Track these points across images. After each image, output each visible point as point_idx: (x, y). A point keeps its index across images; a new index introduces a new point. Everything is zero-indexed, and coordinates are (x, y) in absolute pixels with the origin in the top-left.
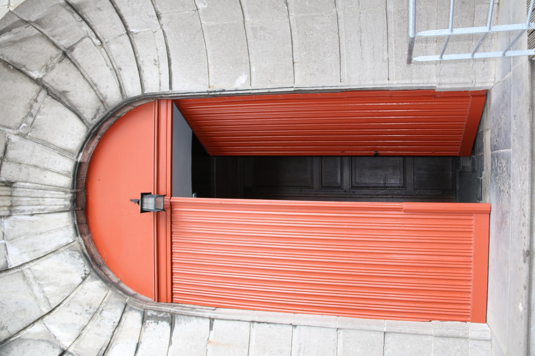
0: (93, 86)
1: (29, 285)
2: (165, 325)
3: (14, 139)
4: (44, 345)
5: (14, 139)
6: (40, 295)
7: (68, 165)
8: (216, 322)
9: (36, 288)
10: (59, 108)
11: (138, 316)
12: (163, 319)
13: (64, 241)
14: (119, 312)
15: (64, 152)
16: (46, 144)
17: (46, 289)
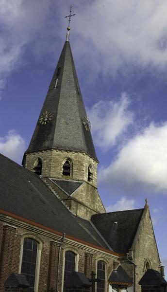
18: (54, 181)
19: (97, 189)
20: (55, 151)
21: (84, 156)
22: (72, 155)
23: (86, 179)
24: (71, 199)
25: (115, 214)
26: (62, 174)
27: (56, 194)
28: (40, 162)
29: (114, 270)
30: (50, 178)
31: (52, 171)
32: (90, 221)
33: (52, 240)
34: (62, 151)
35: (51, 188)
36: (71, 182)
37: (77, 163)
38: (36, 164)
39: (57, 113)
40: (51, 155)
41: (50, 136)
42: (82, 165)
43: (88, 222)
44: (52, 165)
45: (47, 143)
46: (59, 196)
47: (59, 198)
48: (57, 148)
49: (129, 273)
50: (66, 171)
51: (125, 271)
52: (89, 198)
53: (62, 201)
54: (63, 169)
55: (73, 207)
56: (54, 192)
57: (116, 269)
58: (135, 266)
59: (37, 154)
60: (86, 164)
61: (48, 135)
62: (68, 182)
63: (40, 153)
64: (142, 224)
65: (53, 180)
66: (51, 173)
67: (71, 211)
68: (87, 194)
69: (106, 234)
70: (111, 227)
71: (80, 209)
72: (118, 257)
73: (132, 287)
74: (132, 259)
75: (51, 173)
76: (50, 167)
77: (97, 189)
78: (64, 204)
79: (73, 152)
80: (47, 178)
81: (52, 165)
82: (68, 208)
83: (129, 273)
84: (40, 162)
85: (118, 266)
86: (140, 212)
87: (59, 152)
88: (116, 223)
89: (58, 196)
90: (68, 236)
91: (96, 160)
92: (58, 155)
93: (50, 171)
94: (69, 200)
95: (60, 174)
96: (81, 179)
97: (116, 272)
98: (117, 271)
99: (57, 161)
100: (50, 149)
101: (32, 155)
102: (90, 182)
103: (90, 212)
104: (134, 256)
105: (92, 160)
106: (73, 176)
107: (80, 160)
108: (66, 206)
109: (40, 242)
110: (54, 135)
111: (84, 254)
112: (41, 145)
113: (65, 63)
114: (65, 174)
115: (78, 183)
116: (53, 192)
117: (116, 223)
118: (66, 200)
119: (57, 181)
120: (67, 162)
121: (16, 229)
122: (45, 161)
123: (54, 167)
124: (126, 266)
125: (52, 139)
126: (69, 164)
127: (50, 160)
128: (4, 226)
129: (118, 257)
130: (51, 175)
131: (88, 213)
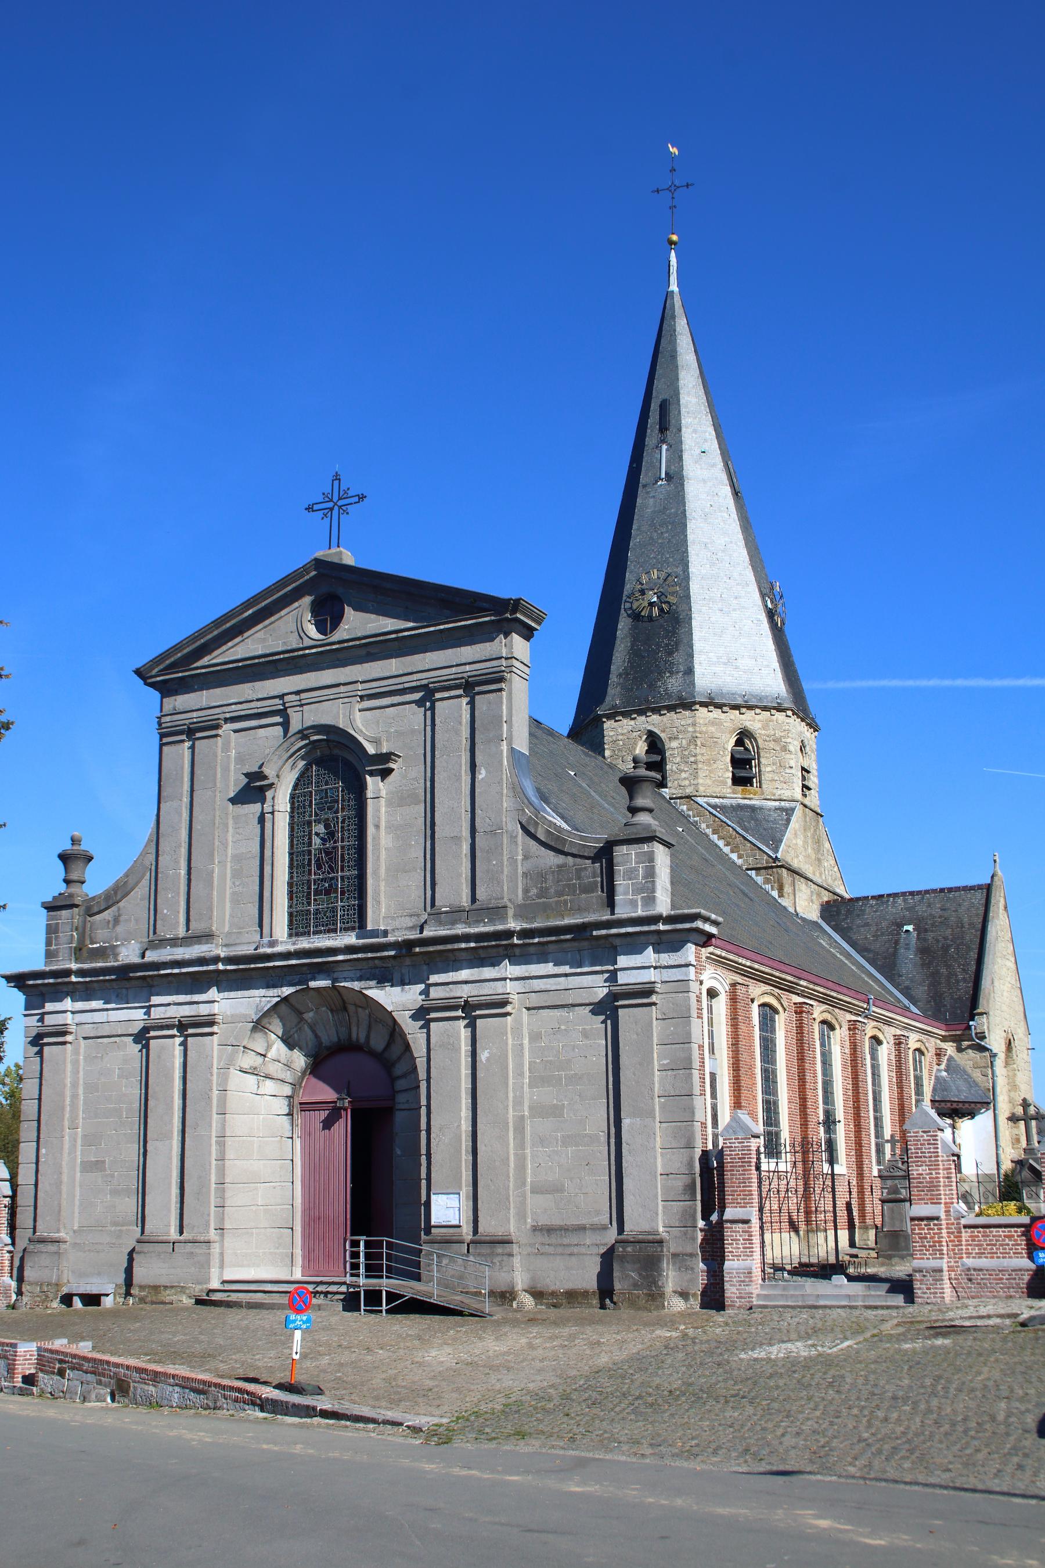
0: (399, 1058)
1: (296, 1026)
2: (286, 1111)
3: (367, 1011)
4: (266, 1044)
5: (367, 1011)
6: (291, 1033)
7: (362, 1040)
8: (290, 1140)
9: (295, 1030)
10: (387, 1038)
11: (290, 1094)
12: (290, 1109)
13: (323, 1041)
14: (290, 1081)
15: (368, 1037)
16: (370, 1027)
17: (296, 1035)
18: (715, 807)
19: (822, 816)
20: (703, 710)
21: (788, 720)
22: (752, 721)
23: (798, 794)
24: (782, 866)
25: (900, 900)
26: (730, 782)
27: (727, 850)
28: (655, 744)
29: (938, 1070)
30: (699, 800)
31: (701, 774)
32: (820, 921)
33: (854, 1018)
34: (725, 709)
35: (709, 831)
36: (761, 808)
37: (772, 745)
38: (641, 748)
39: (687, 578)
40: (694, 725)
41: (678, 657)
42: (784, 749)
43: (816, 923)
44: (699, 758)
45: (673, 684)
46: (740, 857)
47: (740, 862)
48: (710, 703)
49: (977, 1075)
50: (743, 774)
51: (965, 1071)
52: (810, 850)
53: (753, 873)
54: (731, 769)
55: (787, 889)
56: (721, 843)
57: (943, 1067)
58: (994, 1055)
59: (643, 718)
60: (794, 746)
61: (670, 653)
62: (753, 809)
63: (655, 718)
64: (994, 934)
65: (709, 805)
66: (701, 781)
67: (784, 902)
68: (805, 842)
69: (888, 966)
70: (897, 943)
71: (800, 890)
72: (943, 1033)
73: (991, 1112)
74: (985, 1037)
75: (701, 781)
76: (695, 763)
77: (822, 816)
78: (759, 880)
79: (758, 711)
80: (689, 797)
81: (699, 758)
82: (775, 894)
83: (979, 1074)
84: (655, 744)
85: (946, 1057)
86: (979, 897)
87: (716, 713)
88: (910, 928)
89: (734, 856)
90: (878, 1003)
91: (813, 726)
92: (713, 723)
93: (696, 777)
94: (774, 866)
95: (724, 783)
96: (787, 794)
97: (944, 1074)
98: (945, 1071)
99: (713, 742)
100: (686, 704)
101: (626, 724)
102: (807, 801)
103: (819, 895)
104: (988, 1027)
105: (802, 727)
106: (764, 786)
107: (778, 734)
108: (768, 887)
109: (837, 1026)
110: (691, 656)
111: (892, 1038)
112: (652, 686)
113: (681, 383)
114: (737, 781)
115: (781, 809)
116: (716, 845)
117: (910, 928)
118: (765, 868)
119: (723, 808)
120: (739, 742)
121: (812, 1006)
122: (674, 744)
123: (707, 763)
124: (968, 1059)
125: (690, 671)
126: (746, 749)
127: (693, 740)
128: (795, 1004)
129: (943, 1033)
130: (701, 789)
131: (814, 897)
